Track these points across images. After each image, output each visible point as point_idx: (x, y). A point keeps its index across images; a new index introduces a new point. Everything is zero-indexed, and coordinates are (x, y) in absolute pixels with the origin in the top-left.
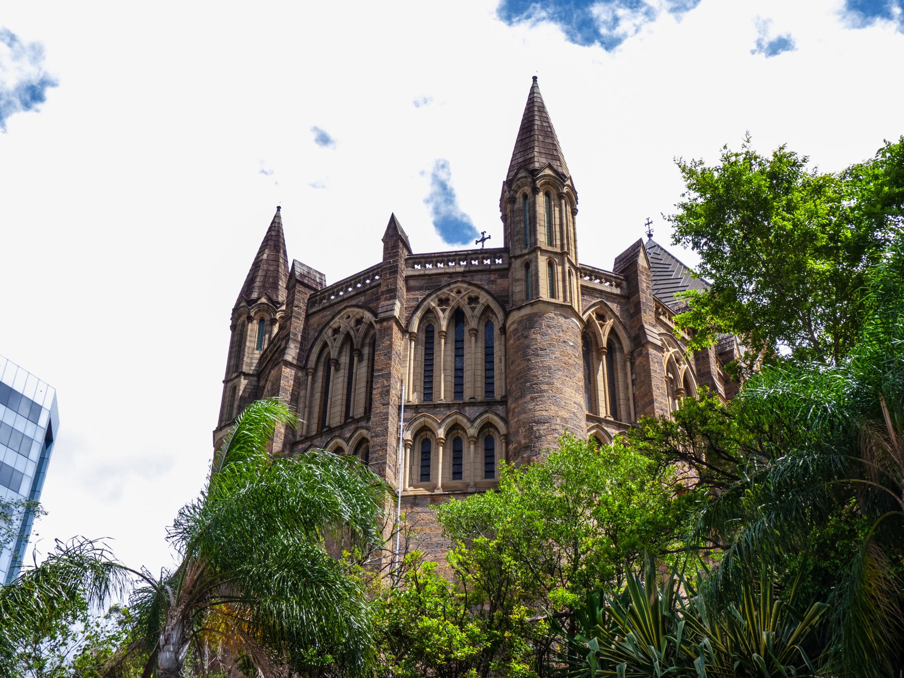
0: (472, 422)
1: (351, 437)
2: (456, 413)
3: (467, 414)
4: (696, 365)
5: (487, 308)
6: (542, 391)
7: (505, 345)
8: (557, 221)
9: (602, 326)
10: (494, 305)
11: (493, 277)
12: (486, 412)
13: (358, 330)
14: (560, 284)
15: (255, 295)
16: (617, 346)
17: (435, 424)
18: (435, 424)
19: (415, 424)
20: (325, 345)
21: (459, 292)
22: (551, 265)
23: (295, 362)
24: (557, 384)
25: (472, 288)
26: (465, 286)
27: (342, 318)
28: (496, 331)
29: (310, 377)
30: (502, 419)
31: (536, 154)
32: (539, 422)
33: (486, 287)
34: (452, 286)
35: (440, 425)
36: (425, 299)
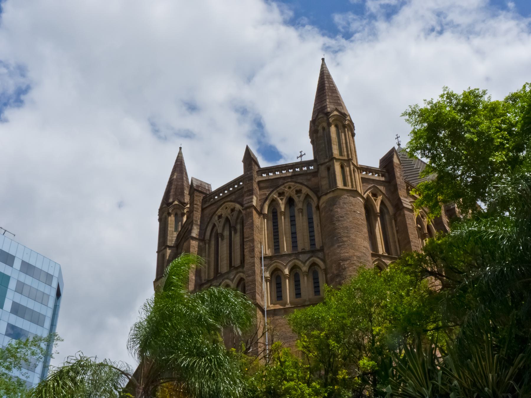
0: (304, 263)
2: (294, 259)
3: (301, 259)
5: (307, 196)
6: (344, 242)
7: (320, 217)
8: (344, 141)
9: (375, 200)
10: (311, 194)
11: (309, 177)
12: (312, 257)
13: (233, 215)
14: (349, 178)
15: (171, 200)
16: (385, 211)
17: (282, 266)
18: (282, 266)
19: (271, 267)
20: (214, 226)
22: (342, 167)
23: (197, 237)
24: (353, 237)
25: (298, 185)
26: (293, 184)
27: (222, 209)
28: (314, 209)
29: (207, 245)
30: (322, 260)
31: (328, 103)
32: (344, 260)
33: (306, 183)
34: (286, 185)
35: (285, 267)
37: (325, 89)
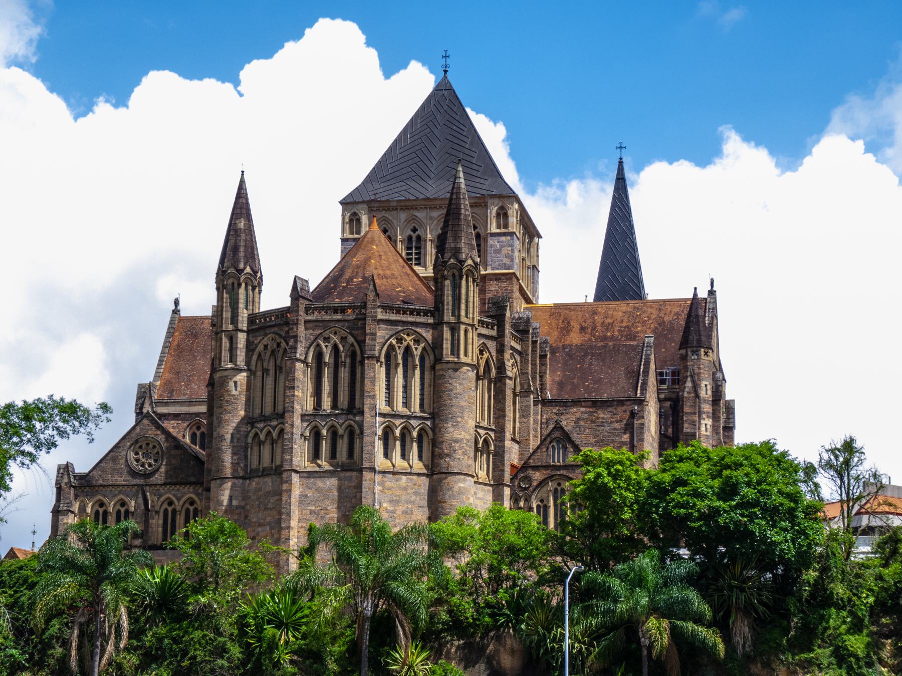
1: (343, 423)
6: (457, 422)
14: (471, 346)
24: (466, 418)
32: (456, 441)
36: (389, 339)
37: (459, 219)
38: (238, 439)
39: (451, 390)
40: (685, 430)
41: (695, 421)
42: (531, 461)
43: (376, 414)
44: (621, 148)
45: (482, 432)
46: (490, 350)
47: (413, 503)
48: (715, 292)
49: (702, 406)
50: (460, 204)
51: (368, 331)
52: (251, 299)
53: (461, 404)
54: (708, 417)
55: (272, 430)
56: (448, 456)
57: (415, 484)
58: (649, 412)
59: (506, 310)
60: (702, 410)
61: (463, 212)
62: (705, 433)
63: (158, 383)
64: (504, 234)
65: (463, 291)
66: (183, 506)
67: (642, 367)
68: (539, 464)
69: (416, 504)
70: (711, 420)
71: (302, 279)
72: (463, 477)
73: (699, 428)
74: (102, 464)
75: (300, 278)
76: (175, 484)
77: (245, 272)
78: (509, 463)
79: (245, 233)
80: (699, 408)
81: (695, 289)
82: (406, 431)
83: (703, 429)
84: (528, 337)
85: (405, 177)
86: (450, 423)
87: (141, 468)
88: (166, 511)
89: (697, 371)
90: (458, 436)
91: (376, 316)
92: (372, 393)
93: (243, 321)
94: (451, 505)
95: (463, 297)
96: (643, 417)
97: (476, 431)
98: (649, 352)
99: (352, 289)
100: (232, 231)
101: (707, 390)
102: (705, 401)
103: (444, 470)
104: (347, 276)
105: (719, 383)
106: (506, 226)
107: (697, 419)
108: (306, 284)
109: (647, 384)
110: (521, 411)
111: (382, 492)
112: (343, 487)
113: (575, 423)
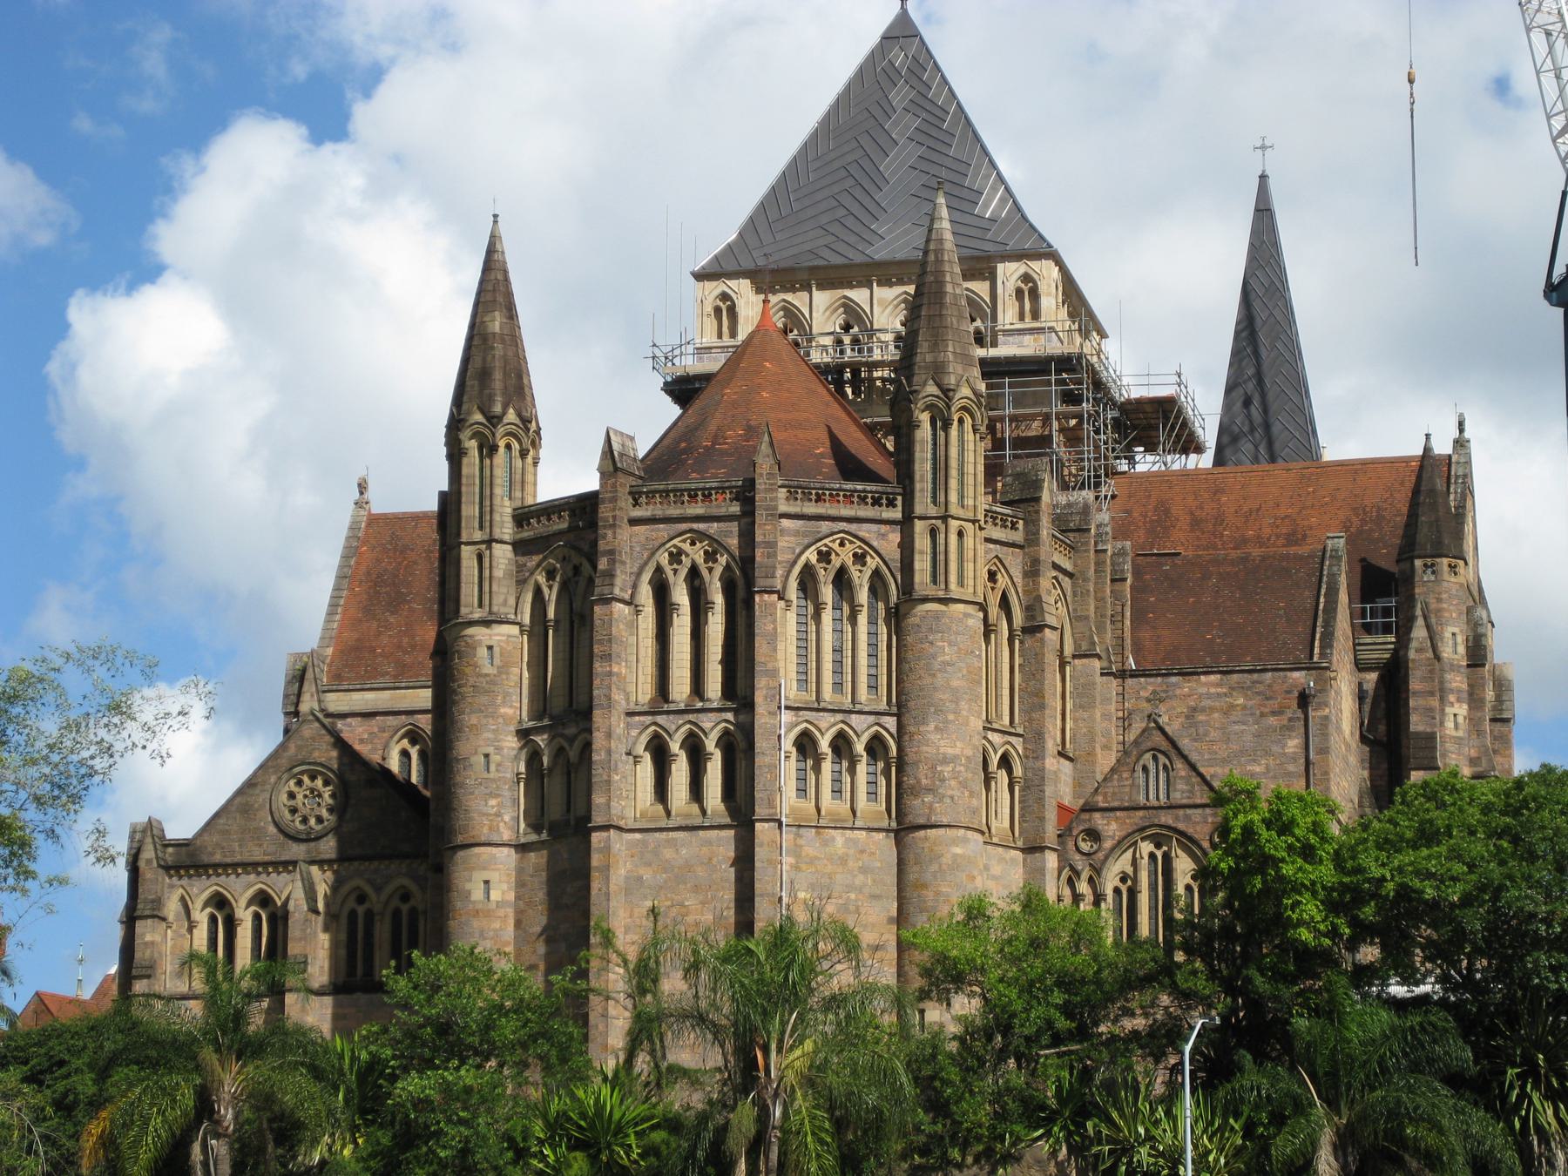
2: (843, 722)
4: (1074, 602)
6: (946, 721)
14: (971, 565)
21: (842, 544)
24: (965, 713)
27: (684, 541)
32: (945, 760)
33: (875, 544)
37: (942, 305)
38: (499, 765)
39: (934, 657)
40: (1412, 728)
41: (1431, 710)
42: (1100, 798)
43: (780, 708)
44: (1263, 148)
45: (996, 738)
46: (1012, 571)
47: (860, 890)
48: (1468, 441)
49: (1448, 676)
50: (943, 273)
51: (759, 538)
52: (518, 477)
53: (955, 683)
54: (1459, 700)
55: (566, 745)
56: (929, 790)
57: (862, 852)
58: (1338, 693)
59: (1040, 488)
60: (1448, 685)
61: (949, 288)
62: (1454, 733)
63: (330, 651)
64: (1031, 331)
65: (954, 452)
66: (387, 903)
67: (1322, 599)
68: (1116, 804)
69: (866, 891)
70: (1465, 706)
71: (622, 434)
72: (962, 831)
73: (1442, 723)
74: (221, 821)
75: (616, 432)
76: (369, 858)
77: (505, 420)
78: (1054, 803)
79: (503, 341)
80: (1442, 682)
81: (1428, 436)
82: (841, 745)
83: (1450, 724)
84: (1087, 543)
85: (824, 219)
86: (932, 726)
87: (301, 827)
88: (353, 913)
89: (1433, 605)
90: (950, 751)
91: (775, 508)
92: (770, 666)
93: (503, 522)
94: (938, 893)
95: (954, 463)
96: (1326, 705)
97: (985, 738)
98: (1335, 569)
99: (723, 453)
100: (477, 339)
101: (1455, 644)
102: (1454, 667)
103: (922, 821)
104: (712, 427)
105: (1481, 630)
106: (1036, 315)
107: (1435, 703)
108: (629, 443)
109: (1332, 634)
110: (1077, 694)
111: (796, 868)
112: (715, 860)
113: (1187, 717)
